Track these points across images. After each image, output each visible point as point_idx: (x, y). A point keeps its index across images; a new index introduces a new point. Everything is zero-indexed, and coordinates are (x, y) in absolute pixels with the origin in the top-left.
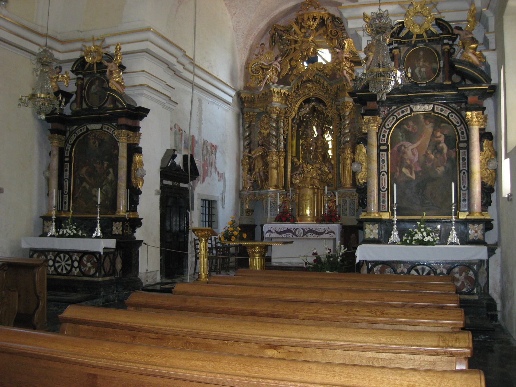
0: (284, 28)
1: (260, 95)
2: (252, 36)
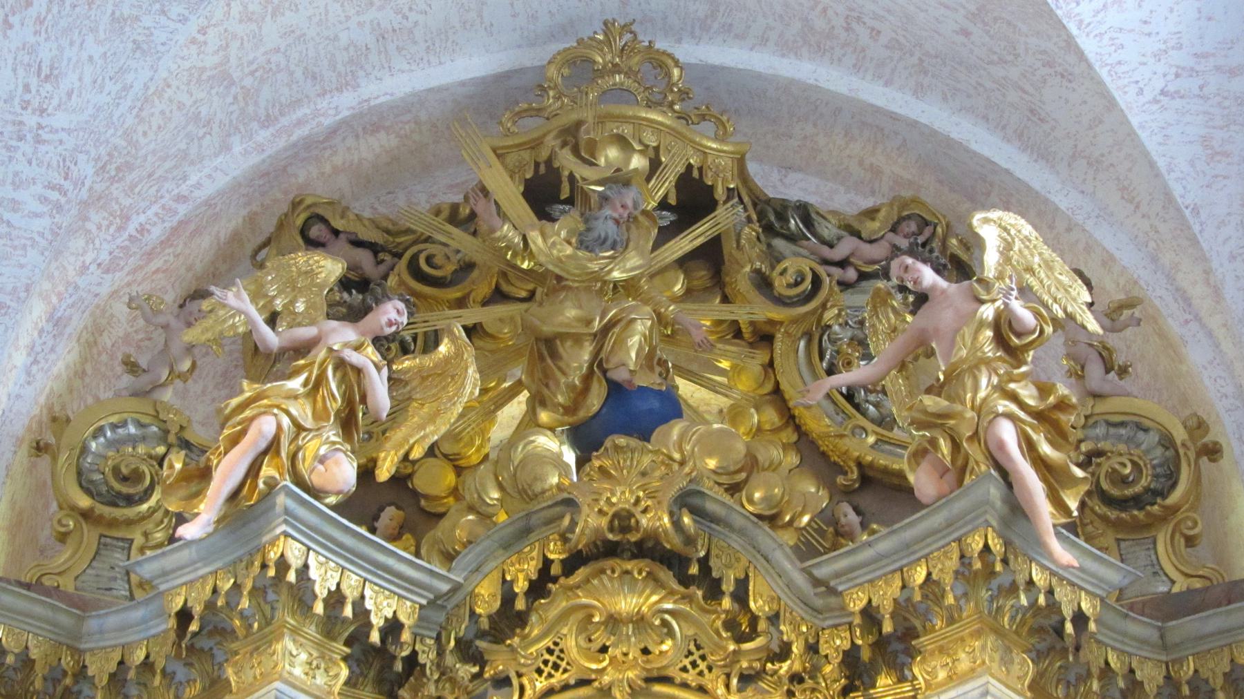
0: (388, 232)
1: (140, 655)
2: (122, 239)
